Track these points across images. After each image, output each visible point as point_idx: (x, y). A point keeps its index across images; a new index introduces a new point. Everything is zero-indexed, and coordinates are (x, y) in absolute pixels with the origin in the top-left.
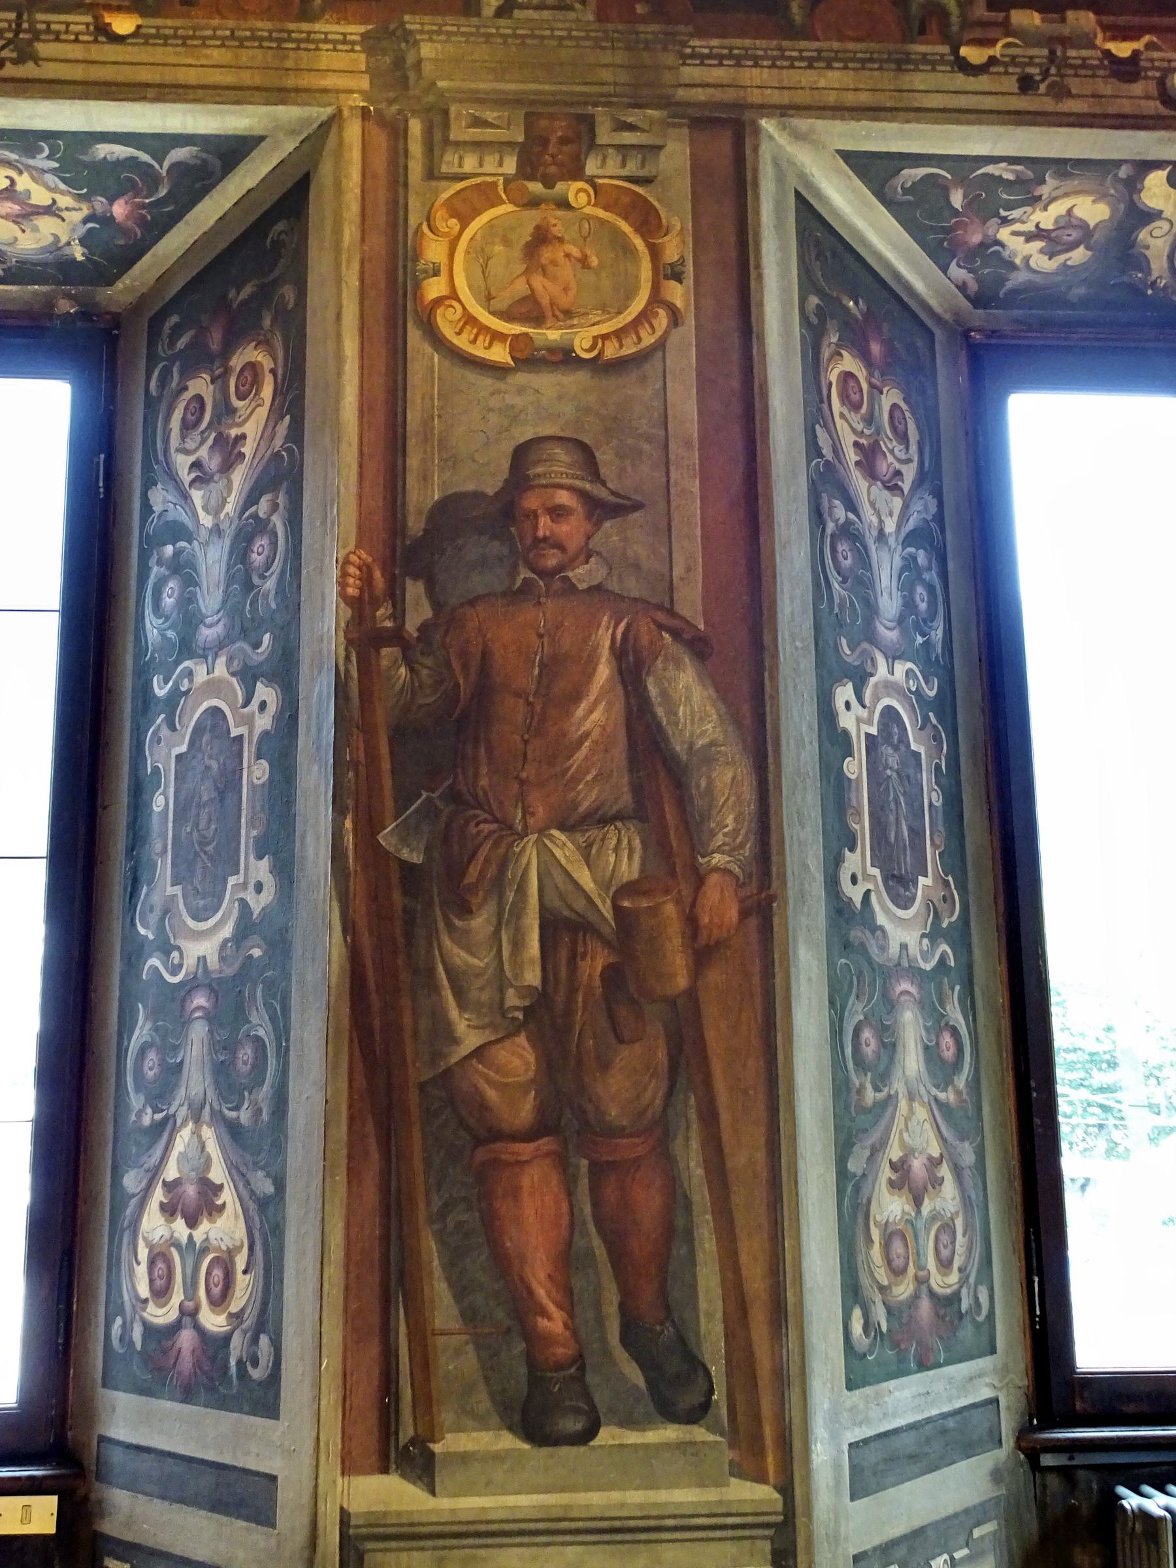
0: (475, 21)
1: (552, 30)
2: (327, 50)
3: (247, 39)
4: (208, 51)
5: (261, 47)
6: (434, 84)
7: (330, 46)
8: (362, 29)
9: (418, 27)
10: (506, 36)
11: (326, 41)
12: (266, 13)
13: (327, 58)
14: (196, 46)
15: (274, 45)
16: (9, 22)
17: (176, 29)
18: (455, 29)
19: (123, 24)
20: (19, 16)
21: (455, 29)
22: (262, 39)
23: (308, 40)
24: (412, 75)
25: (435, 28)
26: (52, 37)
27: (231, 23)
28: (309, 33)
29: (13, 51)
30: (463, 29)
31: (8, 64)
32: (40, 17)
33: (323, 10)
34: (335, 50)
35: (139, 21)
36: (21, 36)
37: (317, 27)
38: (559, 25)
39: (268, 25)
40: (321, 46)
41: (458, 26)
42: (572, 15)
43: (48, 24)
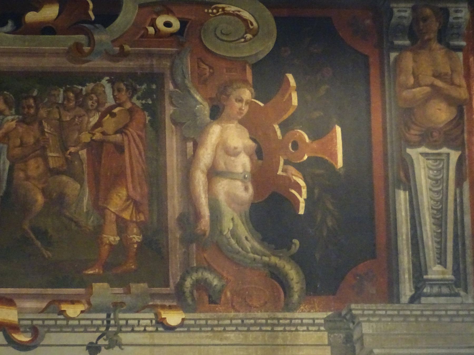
0: (396, 306)
1: (446, 311)
2: (304, 331)
3: (252, 325)
4: (228, 335)
5: (261, 330)
6: (371, 352)
7: (305, 328)
8: (324, 315)
9: (360, 312)
10: (416, 316)
11: (302, 325)
12: (263, 307)
13: (304, 336)
14: (220, 331)
15: (269, 329)
16: (103, 320)
17: (207, 320)
18: (384, 312)
19: (173, 318)
20: (109, 316)
21: (384, 312)
22: (261, 325)
23: (290, 325)
24: (357, 347)
25: (371, 312)
26: (129, 329)
27: (241, 315)
28: (291, 319)
29: (105, 340)
30: (389, 313)
31: (103, 348)
32: (121, 315)
33: (300, 303)
34: (308, 330)
35: (184, 317)
36: (110, 329)
37: (297, 315)
38: (451, 307)
39: (266, 315)
40: (299, 328)
41: (386, 310)
42: (458, 300)
43: (127, 320)
